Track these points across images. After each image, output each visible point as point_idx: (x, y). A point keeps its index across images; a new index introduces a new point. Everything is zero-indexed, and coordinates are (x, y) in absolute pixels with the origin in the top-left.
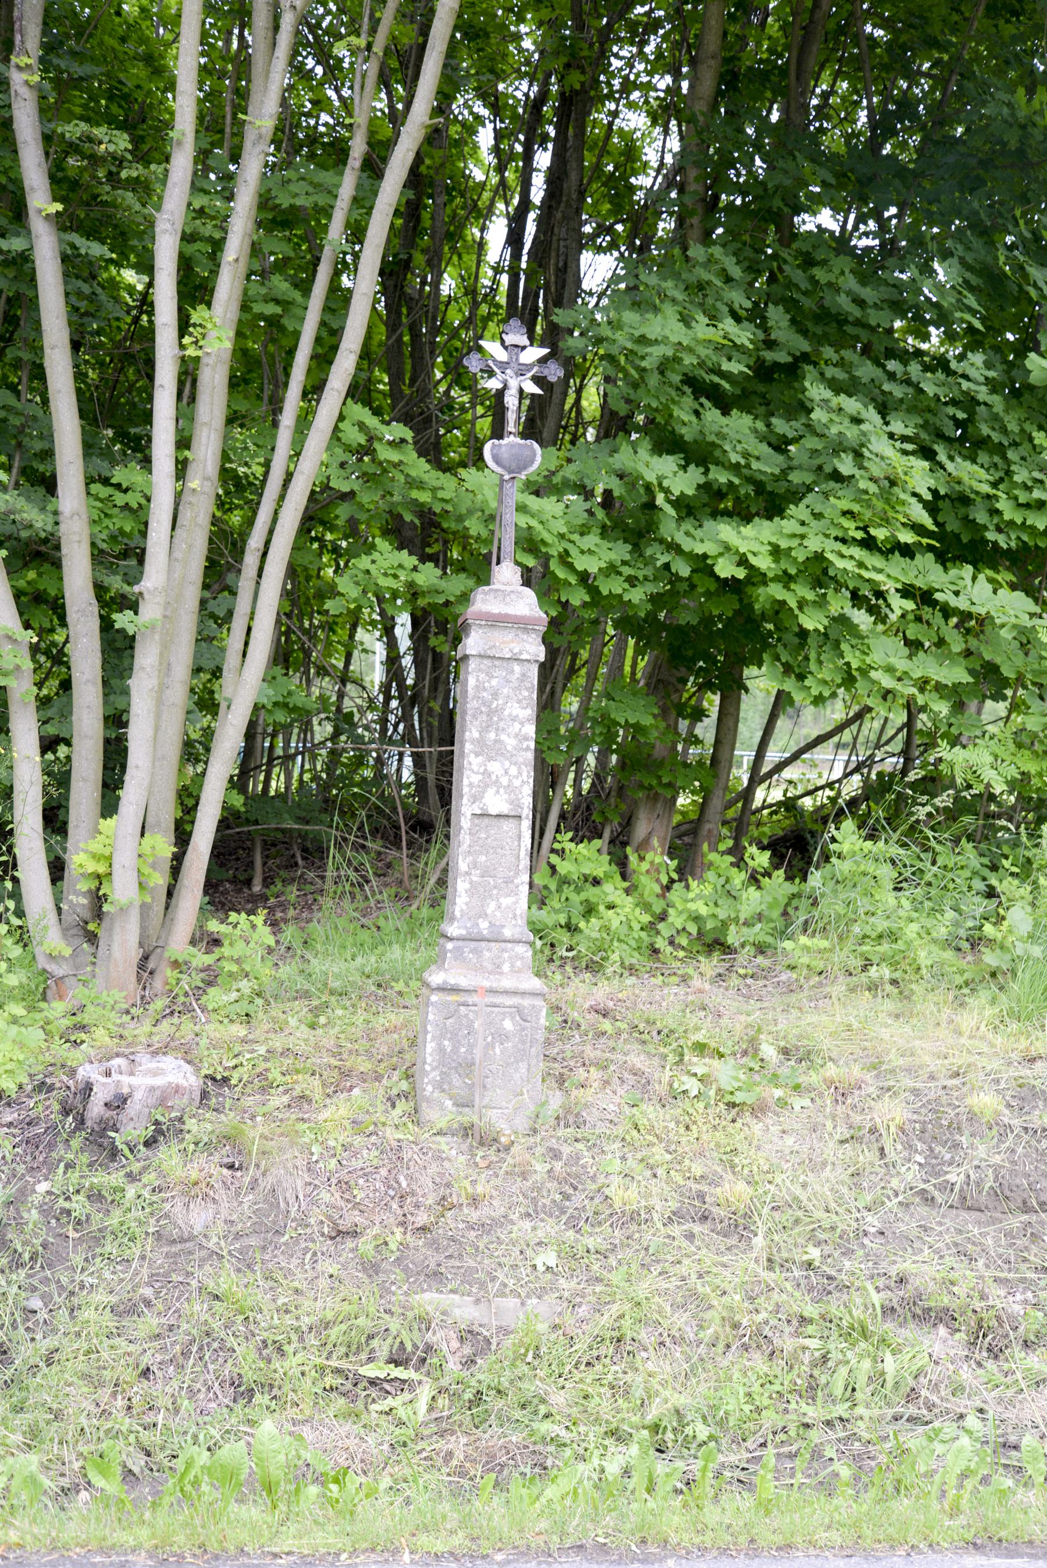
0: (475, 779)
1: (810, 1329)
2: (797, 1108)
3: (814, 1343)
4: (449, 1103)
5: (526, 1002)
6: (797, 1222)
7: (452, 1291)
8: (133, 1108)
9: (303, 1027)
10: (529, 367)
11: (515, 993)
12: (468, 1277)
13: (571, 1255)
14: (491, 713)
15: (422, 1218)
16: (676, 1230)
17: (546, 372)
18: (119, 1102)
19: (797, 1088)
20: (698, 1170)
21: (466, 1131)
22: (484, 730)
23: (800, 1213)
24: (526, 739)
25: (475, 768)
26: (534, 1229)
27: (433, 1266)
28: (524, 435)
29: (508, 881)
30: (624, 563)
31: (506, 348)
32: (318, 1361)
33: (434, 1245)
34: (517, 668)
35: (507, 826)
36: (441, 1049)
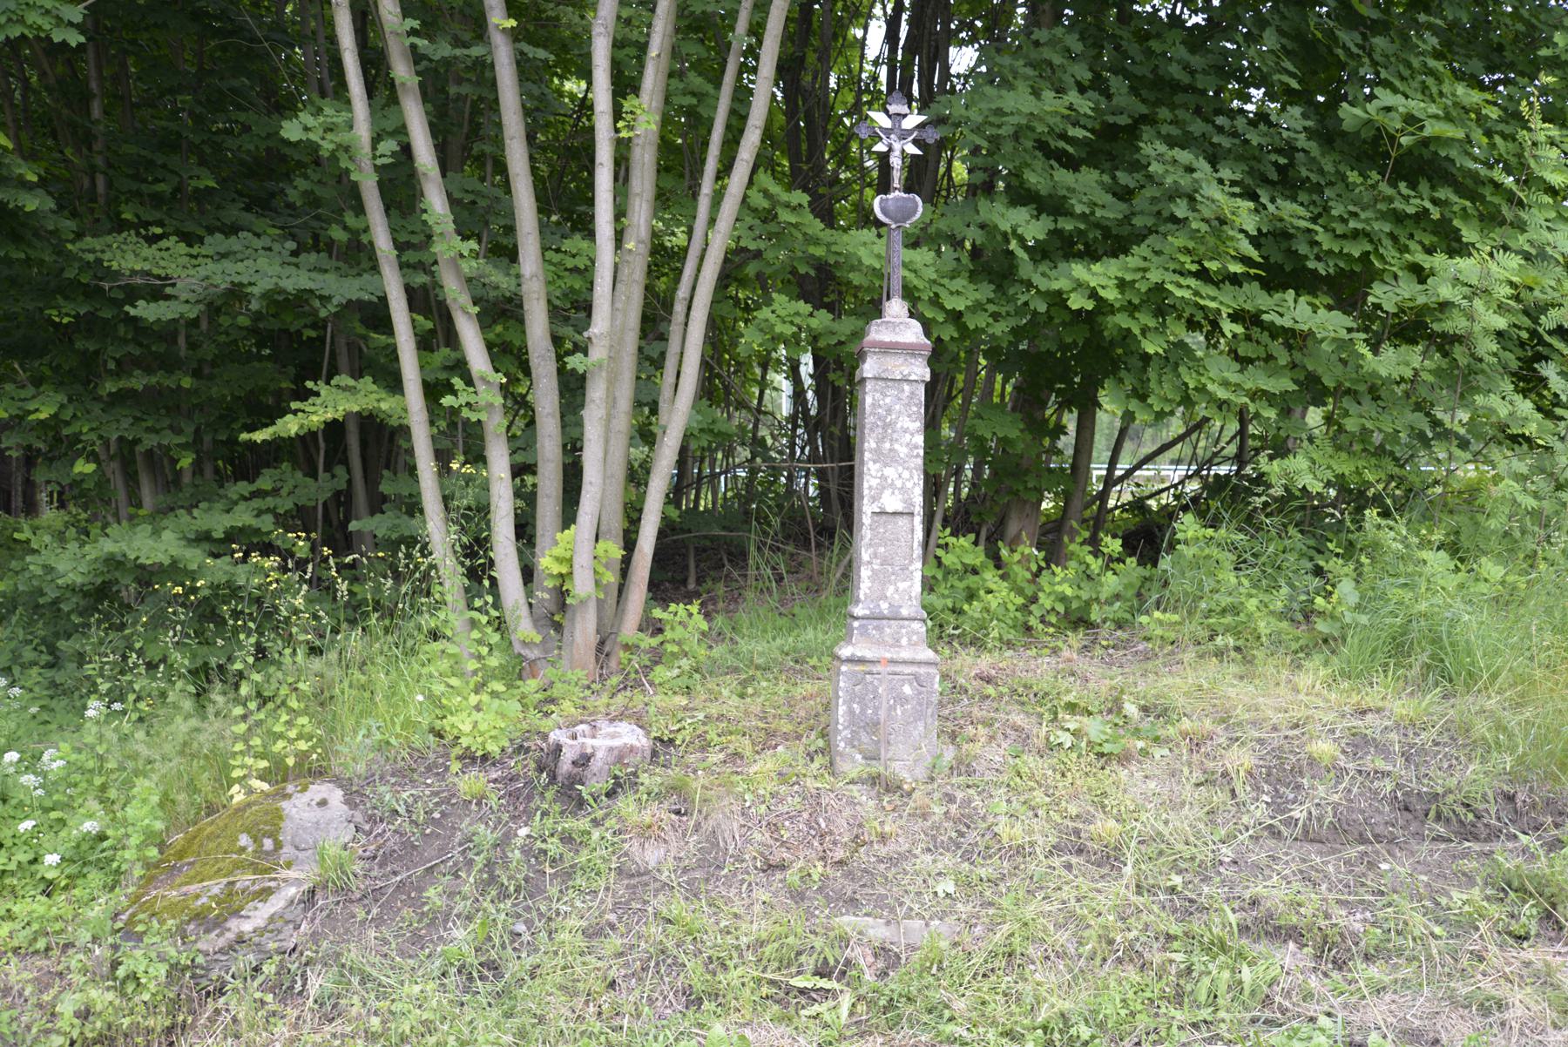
0: (874, 482)
1: (1176, 945)
2: (1157, 757)
3: (1179, 957)
4: (859, 757)
5: (922, 670)
6: (1161, 853)
7: (867, 915)
8: (596, 764)
9: (734, 697)
10: (910, 132)
11: (912, 663)
12: (880, 903)
13: (966, 884)
14: (886, 426)
15: (839, 854)
16: (1056, 861)
17: (924, 136)
18: (584, 760)
19: (1156, 739)
20: (1073, 810)
21: (874, 780)
22: (880, 441)
23: (1163, 846)
24: (916, 447)
25: (873, 473)
26: (934, 861)
27: (849, 893)
28: (907, 190)
29: (904, 568)
30: (989, 301)
31: (890, 117)
32: (756, 974)
33: (850, 875)
34: (906, 387)
35: (902, 522)
36: (851, 712)
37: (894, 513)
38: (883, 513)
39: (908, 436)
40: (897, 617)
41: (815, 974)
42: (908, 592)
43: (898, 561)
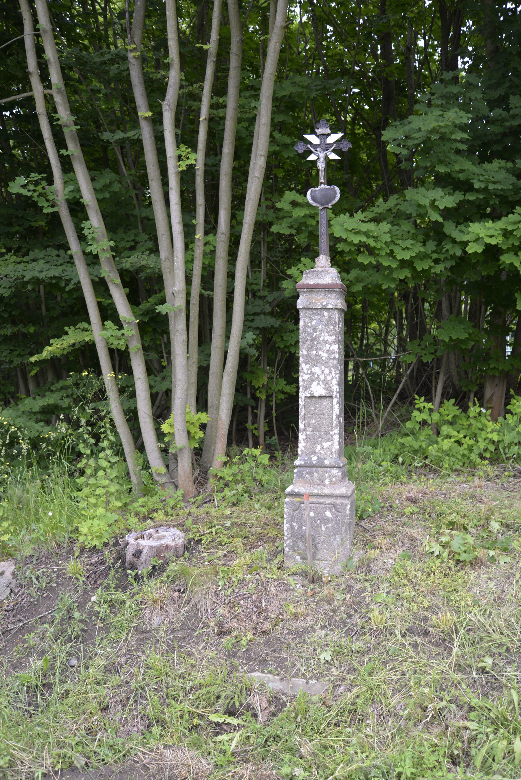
0: (306, 377)
1: (472, 715)
2: (502, 563)
3: (472, 725)
4: (298, 558)
5: (338, 501)
6: (481, 639)
7: (270, 672)
8: (144, 556)
9: (263, 509)
10: (331, 145)
11: (331, 496)
12: (281, 664)
13: (338, 652)
14: (313, 340)
15: (267, 626)
16: (406, 641)
17: (341, 146)
18: (138, 553)
19: (505, 550)
20: (426, 604)
21: (304, 574)
22: (309, 350)
23: (483, 635)
24: (333, 352)
25: (305, 371)
26: (326, 635)
27: (264, 655)
28: (329, 183)
29: (327, 433)
30: (433, 252)
31: (318, 136)
32: (190, 709)
33: (268, 643)
34: (326, 313)
35: (325, 402)
36: (292, 528)
37: (320, 397)
38: (312, 397)
39: (328, 346)
40: (321, 465)
41: (225, 713)
42: (329, 448)
43: (324, 428)
